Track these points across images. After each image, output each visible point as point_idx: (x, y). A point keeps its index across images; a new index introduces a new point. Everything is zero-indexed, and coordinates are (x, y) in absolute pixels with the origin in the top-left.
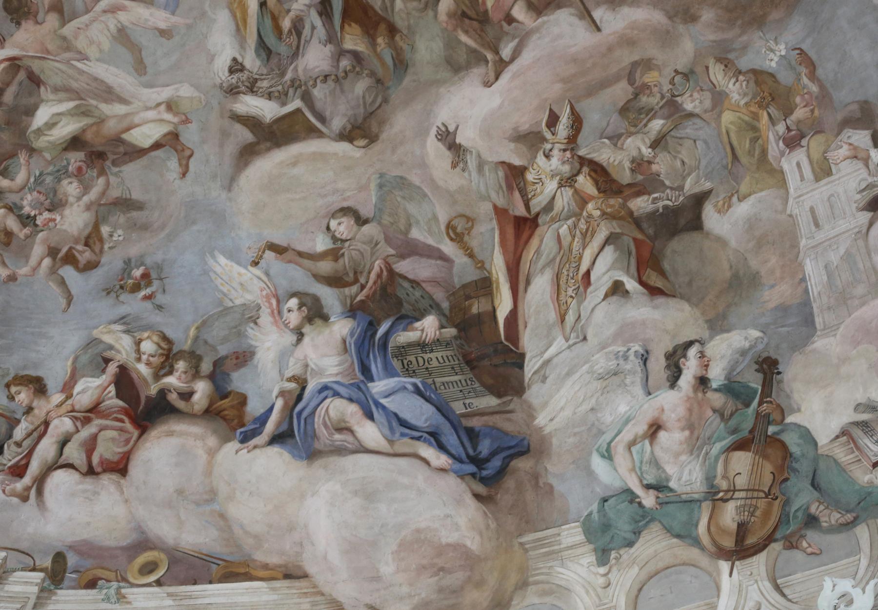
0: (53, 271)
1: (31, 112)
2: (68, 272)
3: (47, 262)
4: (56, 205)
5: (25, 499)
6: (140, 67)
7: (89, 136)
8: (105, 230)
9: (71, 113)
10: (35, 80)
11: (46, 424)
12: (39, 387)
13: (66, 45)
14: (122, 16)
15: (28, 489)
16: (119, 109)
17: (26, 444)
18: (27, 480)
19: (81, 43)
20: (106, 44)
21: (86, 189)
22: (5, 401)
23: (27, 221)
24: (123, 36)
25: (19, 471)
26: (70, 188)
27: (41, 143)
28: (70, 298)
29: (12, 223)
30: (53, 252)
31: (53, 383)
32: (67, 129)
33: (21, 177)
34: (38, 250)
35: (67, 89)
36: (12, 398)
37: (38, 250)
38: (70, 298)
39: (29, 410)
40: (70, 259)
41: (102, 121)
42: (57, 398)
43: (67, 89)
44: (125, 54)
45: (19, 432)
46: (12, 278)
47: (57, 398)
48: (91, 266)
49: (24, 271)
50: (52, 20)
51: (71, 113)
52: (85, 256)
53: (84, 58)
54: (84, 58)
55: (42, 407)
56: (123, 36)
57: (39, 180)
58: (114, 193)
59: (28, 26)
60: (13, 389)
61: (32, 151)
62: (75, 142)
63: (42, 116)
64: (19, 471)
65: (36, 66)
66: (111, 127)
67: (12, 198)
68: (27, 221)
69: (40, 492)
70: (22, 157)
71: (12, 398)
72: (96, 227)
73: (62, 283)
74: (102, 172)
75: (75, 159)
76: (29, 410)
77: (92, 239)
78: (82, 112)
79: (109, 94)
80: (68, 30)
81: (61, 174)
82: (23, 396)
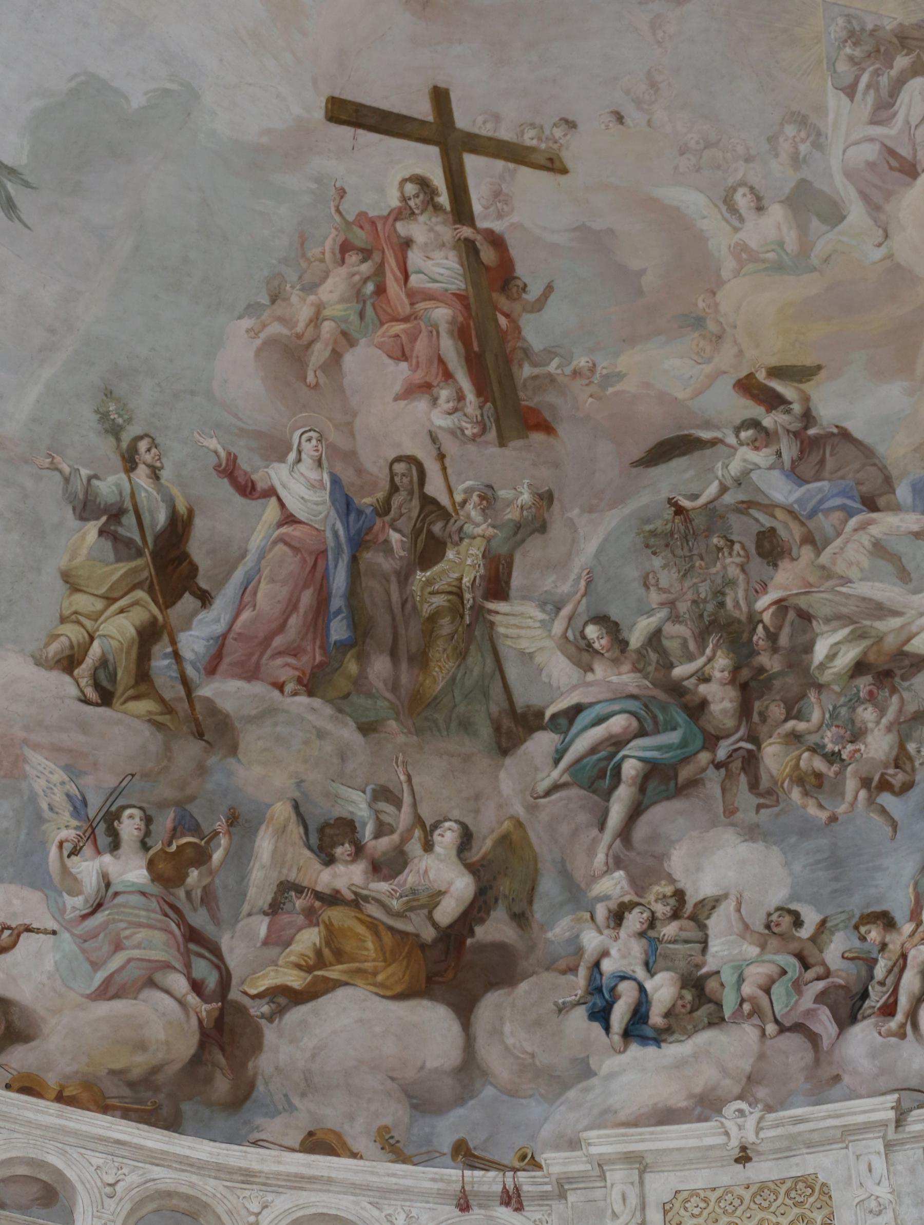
0: (871, 801)
1: (809, 648)
2: (886, 799)
3: (863, 794)
4: (857, 735)
5: (903, 1036)
6: (904, 576)
7: (872, 658)
8: (911, 747)
9: (848, 640)
10: (805, 617)
11: (904, 956)
12: (887, 921)
13: (826, 573)
14: (874, 530)
15: (903, 1026)
16: (895, 622)
17: (890, 981)
18: (900, 1017)
19: (840, 568)
20: (865, 562)
21: (882, 711)
22: (857, 943)
23: (833, 758)
24: (879, 549)
25: (889, 1010)
26: (867, 714)
27: (827, 677)
28: (894, 825)
29: (819, 764)
30: (866, 783)
31: (900, 913)
32: (848, 656)
33: (816, 716)
34: (851, 784)
35: (838, 617)
36: (863, 939)
37: (851, 784)
38: (894, 825)
39: (884, 947)
40: (885, 785)
41: (880, 639)
42: (908, 928)
43: (838, 617)
44: (886, 567)
45: (880, 971)
46: (833, 819)
47: (908, 928)
48: (907, 787)
49: (842, 809)
50: (807, 553)
51: (848, 640)
52: (898, 779)
53: (847, 581)
54: (847, 581)
55: (895, 941)
56: (879, 549)
57: (834, 715)
58: (911, 708)
59: (785, 565)
60: (863, 930)
61: (820, 687)
62: (859, 668)
63: (821, 650)
64: (889, 1010)
65: (802, 602)
66: (891, 642)
67: (812, 739)
68: (833, 758)
69: (915, 1026)
70: (812, 696)
71: (863, 939)
72: (902, 747)
73: (883, 811)
74: (894, 690)
75: (864, 683)
76: (884, 947)
77: (901, 759)
78: (859, 635)
79: (881, 610)
80: (824, 558)
81: (854, 702)
82: (874, 934)
